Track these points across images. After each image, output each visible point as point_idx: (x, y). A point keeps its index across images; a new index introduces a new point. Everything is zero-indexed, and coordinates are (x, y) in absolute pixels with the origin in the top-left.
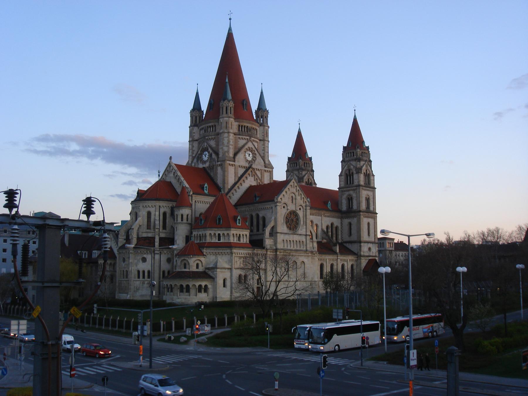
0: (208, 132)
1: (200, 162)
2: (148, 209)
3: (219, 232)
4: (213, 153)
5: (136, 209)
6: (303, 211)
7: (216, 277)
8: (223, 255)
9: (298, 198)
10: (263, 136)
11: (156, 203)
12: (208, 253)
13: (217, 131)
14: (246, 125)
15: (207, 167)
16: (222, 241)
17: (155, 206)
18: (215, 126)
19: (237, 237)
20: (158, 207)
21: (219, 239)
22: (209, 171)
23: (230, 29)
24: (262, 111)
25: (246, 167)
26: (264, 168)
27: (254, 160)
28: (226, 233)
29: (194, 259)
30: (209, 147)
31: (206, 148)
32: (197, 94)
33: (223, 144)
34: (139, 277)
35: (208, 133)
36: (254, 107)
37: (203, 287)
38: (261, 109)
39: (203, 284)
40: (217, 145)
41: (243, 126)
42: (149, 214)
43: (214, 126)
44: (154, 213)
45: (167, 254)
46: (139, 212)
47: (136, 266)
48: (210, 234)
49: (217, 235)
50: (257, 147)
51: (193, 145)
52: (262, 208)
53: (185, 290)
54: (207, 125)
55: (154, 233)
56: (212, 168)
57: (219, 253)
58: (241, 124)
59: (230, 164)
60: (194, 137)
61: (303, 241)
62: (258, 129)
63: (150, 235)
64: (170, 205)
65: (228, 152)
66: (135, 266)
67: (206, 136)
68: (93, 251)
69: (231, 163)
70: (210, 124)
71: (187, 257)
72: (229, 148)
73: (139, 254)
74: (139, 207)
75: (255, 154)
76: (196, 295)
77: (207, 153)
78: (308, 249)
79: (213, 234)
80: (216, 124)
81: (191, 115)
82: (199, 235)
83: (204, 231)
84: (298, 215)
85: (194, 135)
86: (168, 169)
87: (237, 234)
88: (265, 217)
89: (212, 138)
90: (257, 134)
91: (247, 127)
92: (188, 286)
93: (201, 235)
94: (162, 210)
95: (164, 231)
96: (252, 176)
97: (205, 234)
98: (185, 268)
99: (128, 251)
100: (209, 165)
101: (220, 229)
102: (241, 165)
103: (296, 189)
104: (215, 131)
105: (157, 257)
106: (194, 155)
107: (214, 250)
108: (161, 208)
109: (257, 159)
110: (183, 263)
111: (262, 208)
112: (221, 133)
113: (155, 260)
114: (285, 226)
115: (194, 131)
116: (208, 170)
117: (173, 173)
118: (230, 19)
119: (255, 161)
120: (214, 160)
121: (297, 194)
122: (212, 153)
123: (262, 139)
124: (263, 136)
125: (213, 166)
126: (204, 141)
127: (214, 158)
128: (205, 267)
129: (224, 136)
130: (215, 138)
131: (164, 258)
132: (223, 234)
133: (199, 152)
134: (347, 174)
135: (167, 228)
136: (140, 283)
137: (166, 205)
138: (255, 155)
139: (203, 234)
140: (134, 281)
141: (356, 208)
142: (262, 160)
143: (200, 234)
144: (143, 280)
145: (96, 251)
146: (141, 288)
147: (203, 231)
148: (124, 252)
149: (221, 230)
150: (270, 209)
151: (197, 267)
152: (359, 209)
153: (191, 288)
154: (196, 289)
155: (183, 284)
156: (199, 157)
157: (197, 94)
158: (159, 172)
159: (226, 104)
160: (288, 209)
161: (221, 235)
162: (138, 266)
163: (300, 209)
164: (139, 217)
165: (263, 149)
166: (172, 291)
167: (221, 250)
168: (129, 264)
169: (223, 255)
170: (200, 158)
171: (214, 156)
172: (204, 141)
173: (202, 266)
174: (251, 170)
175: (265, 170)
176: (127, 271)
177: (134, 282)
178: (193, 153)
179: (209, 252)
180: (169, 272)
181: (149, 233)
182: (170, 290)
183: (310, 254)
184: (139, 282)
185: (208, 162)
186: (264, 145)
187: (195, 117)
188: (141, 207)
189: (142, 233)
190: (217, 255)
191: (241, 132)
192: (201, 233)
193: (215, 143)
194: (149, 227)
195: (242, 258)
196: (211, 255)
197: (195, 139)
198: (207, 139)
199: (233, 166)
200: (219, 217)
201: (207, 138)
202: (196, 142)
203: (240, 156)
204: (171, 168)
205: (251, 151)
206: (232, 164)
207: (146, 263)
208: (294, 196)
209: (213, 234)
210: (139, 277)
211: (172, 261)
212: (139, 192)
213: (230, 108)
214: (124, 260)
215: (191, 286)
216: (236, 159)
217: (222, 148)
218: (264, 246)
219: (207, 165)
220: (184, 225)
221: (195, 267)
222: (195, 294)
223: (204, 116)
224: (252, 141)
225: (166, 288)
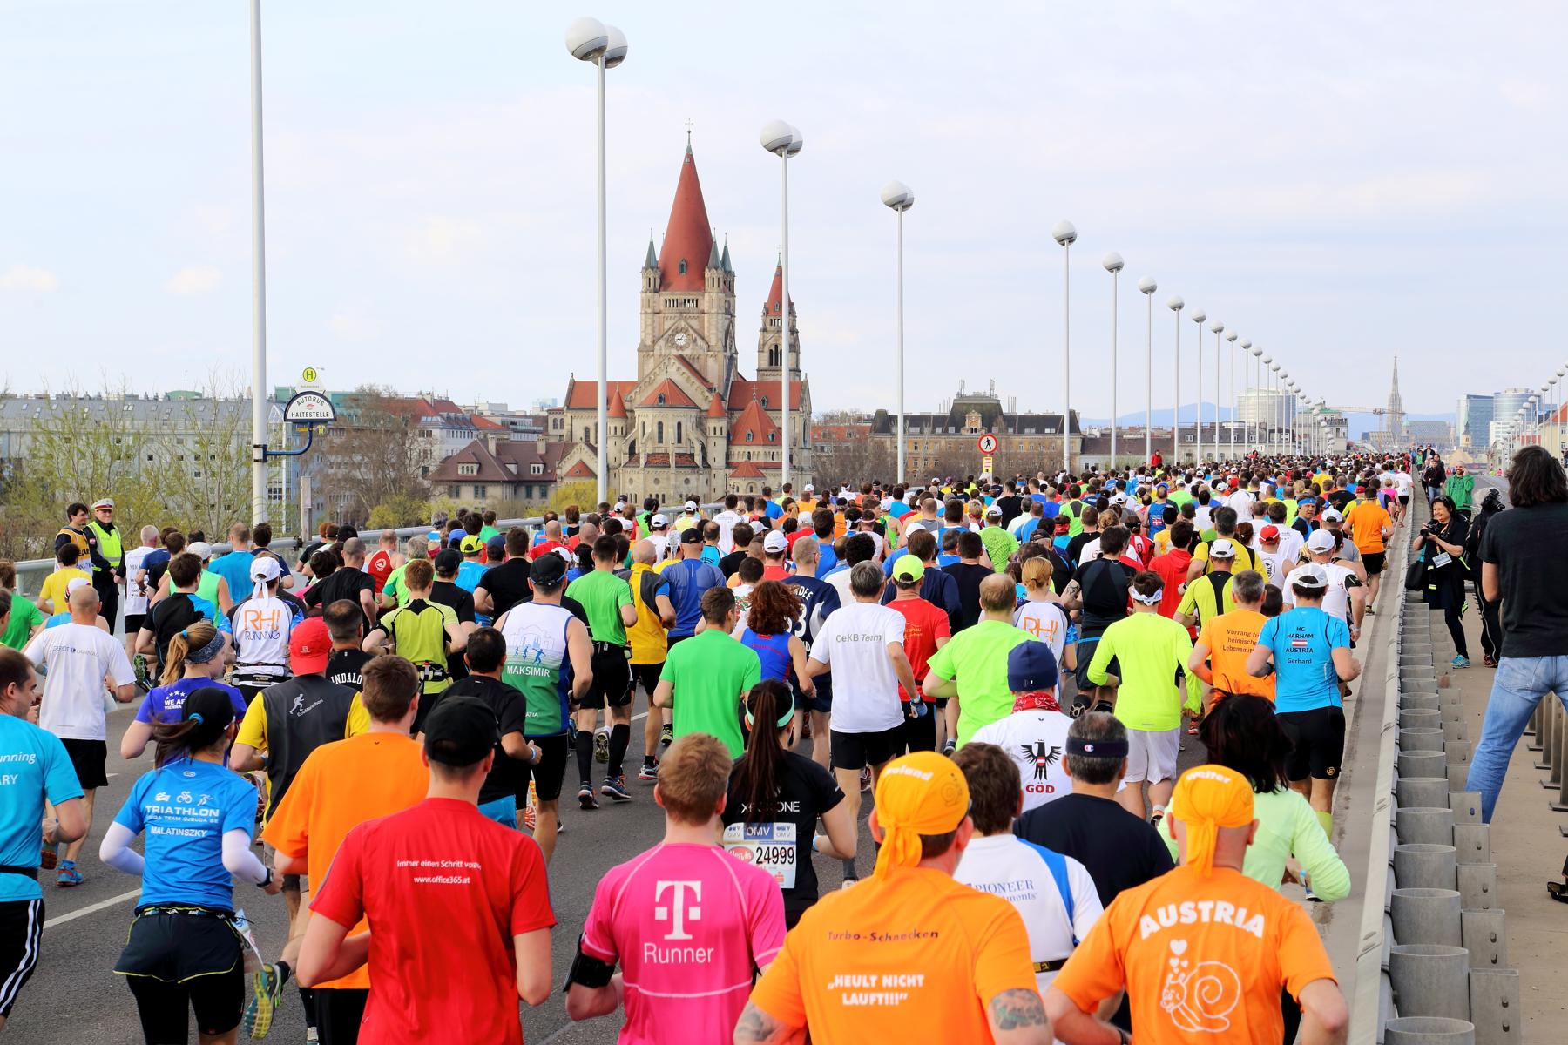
13: (700, 307)
22: (691, 362)
23: (689, 149)
32: (652, 243)
38: (730, 272)
42: (679, 425)
54: (683, 297)
63: (682, 451)
68: (532, 466)
116: (687, 358)
133: (670, 332)
134: (771, 351)
157: (652, 243)
171: (699, 341)
194: (679, 441)
204: (673, 361)
219: (686, 353)
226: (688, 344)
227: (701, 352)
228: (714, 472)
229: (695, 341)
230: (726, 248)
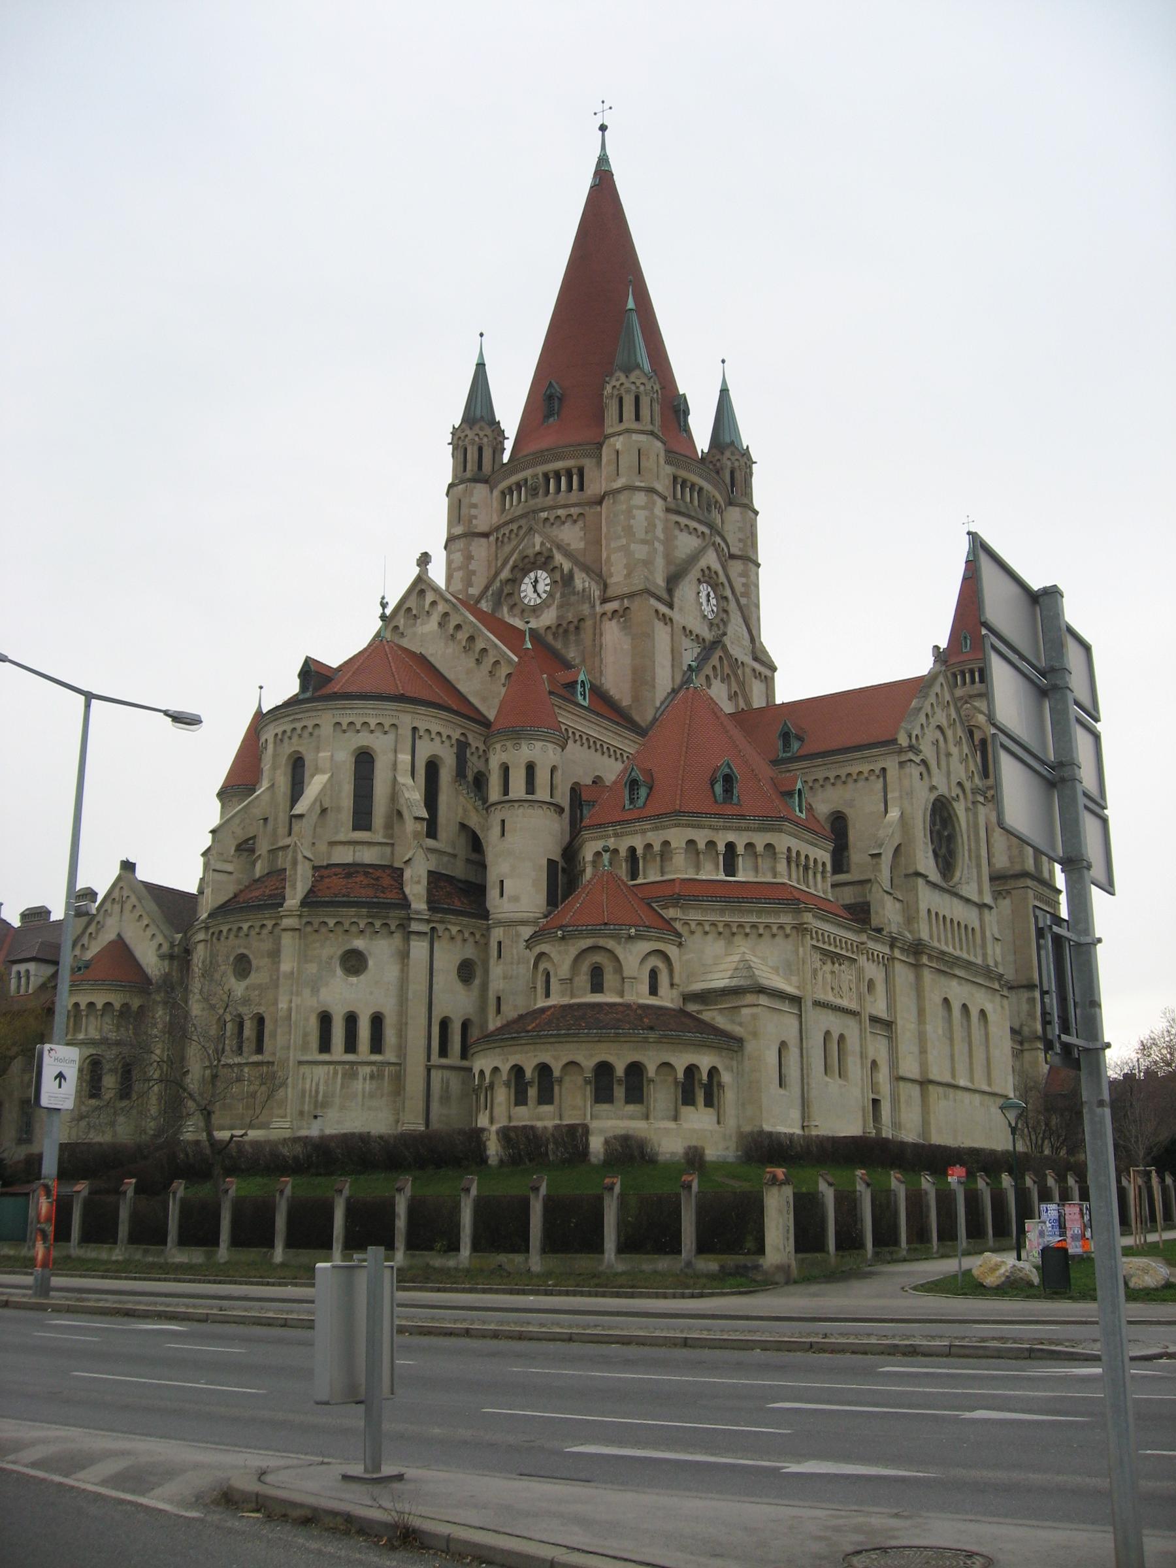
0: (547, 492)
1: (512, 607)
2: (364, 739)
3: (731, 837)
4: (576, 570)
5: (295, 739)
6: (967, 809)
7: (755, 1034)
8: (760, 935)
9: (954, 750)
10: (740, 540)
11: (401, 715)
12: (693, 925)
15: (549, 628)
16: (740, 877)
17: (393, 725)
19: (797, 866)
20: (409, 733)
21: (730, 869)
22: (558, 645)
23: (603, 160)
24: (733, 454)
25: (703, 640)
26: (748, 660)
27: (722, 620)
28: (760, 840)
29: (645, 947)
30: (559, 547)
31: (539, 553)
33: (629, 531)
34: (325, 1045)
35: (550, 497)
36: (702, 437)
37: (705, 1077)
38: (732, 443)
39: (705, 1061)
40: (596, 542)
41: (689, 484)
42: (364, 761)
43: (575, 471)
44: (391, 756)
45: (459, 938)
46: (318, 749)
47: (315, 991)
48: (691, 842)
49: (721, 848)
51: (470, 552)
52: (832, 775)
53: (619, 1092)
54: (541, 469)
55: (388, 849)
56: (572, 627)
57: (741, 926)
58: (683, 474)
59: (657, 611)
60: (474, 522)
61: (973, 929)
63: (368, 856)
64: (456, 735)
65: (648, 563)
66: (307, 992)
67: (543, 510)
68: (15, 968)
69: (663, 609)
70: (560, 465)
71: (612, 936)
72: (655, 550)
73: (331, 935)
74: (316, 732)
75: (726, 598)
76: (676, 1118)
77: (542, 575)
78: (991, 963)
79: (701, 845)
80: (588, 464)
82: (623, 853)
83: (653, 830)
84: (955, 819)
85: (473, 512)
86: (412, 603)
87: (798, 853)
88: (847, 811)
89: (570, 515)
91: (701, 489)
92: (635, 1070)
93: (640, 852)
94: (425, 750)
95: (430, 842)
96: (723, 681)
97: (666, 843)
98: (597, 987)
99: (270, 924)
100: (558, 617)
101: (735, 822)
102: (689, 627)
103: (949, 716)
104: (581, 488)
105: (419, 948)
106: (474, 591)
107: (722, 912)
108: (420, 737)
109: (733, 621)
110: (585, 967)
111: (832, 775)
112: (618, 491)
113: (411, 963)
114: (930, 854)
115: (474, 500)
116: (550, 638)
117: (435, 618)
118: (603, 128)
119: (725, 623)
120: (585, 596)
121: (949, 733)
122: (571, 571)
124: (740, 540)
125: (581, 620)
126: (531, 529)
127: (584, 590)
128: (681, 989)
129: (633, 502)
130: (581, 514)
131: (448, 957)
132: (750, 846)
133: (505, 574)
135: (442, 833)
136: (336, 1073)
137: (442, 730)
138: (725, 604)
139: (649, 846)
140: (300, 1063)
141: (1008, 865)
142: (745, 628)
143: (632, 850)
144: (350, 1057)
145: (32, 966)
146: (337, 1101)
147: (649, 834)
148: (245, 926)
149: (739, 829)
150: (873, 778)
151: (654, 991)
152: (1018, 868)
153: (652, 1081)
154: (676, 1082)
155: (611, 1059)
156: (506, 592)
157: (481, 366)
158: (384, 605)
159: (638, 384)
160: (933, 788)
161: (740, 849)
162: (323, 991)
163: (958, 796)
164: (313, 776)
165: (743, 590)
166: (546, 1097)
167: (750, 912)
168: (276, 985)
169: (760, 935)
170: (510, 595)
171: (581, 581)
172: (531, 529)
173: (672, 985)
174: (719, 653)
175: (754, 670)
176: (260, 1021)
177: (304, 1069)
178: (469, 584)
179: (700, 923)
180: (465, 1026)
181: (365, 848)
182: (532, 1092)
183: (997, 986)
184: (326, 1067)
185: (554, 607)
186: (745, 574)
187: (476, 448)
188: (327, 729)
189: (332, 844)
190: (734, 934)
191: (680, 502)
192: (638, 843)
193: (582, 534)
194: (362, 818)
195: (829, 962)
196: (706, 933)
197: (476, 531)
198: (547, 519)
199: (666, 624)
200: (727, 770)
201: (544, 515)
202: (483, 541)
203: (686, 591)
204: (430, 597)
205: (715, 586)
206: (663, 615)
207: (362, 977)
208: (941, 739)
209: (701, 845)
210: (325, 1045)
211: (479, 972)
212: (313, 668)
214: (243, 966)
215: (651, 1070)
216: (676, 600)
217: (625, 549)
218: (875, 922)
219: (548, 618)
220: (540, 811)
221: (645, 988)
222: (673, 1113)
223: (509, 445)
225: (507, 1084)
226: (551, 595)
227: (585, 609)
228: (497, 934)
229: (568, 580)
230: (724, 392)
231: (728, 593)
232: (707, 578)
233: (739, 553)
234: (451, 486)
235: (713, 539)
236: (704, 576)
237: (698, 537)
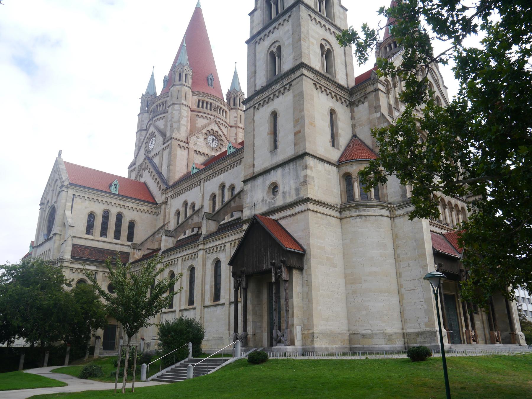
14: (210, 101)
18: (166, 102)
32: (153, 76)
43: (164, 103)
50: (225, 133)
62: (228, 111)
65: (178, 130)
69: (182, 144)
81: (142, 100)
90: (226, 117)
102: (198, 150)
123: (233, 125)
133: (145, 141)
198: (155, 120)
213: (186, 75)
224: (219, 123)
231: (223, 138)
232: (212, 133)
233: (234, 125)
234: (138, 115)
235: (215, 120)
236: (210, 133)
237: (208, 119)
